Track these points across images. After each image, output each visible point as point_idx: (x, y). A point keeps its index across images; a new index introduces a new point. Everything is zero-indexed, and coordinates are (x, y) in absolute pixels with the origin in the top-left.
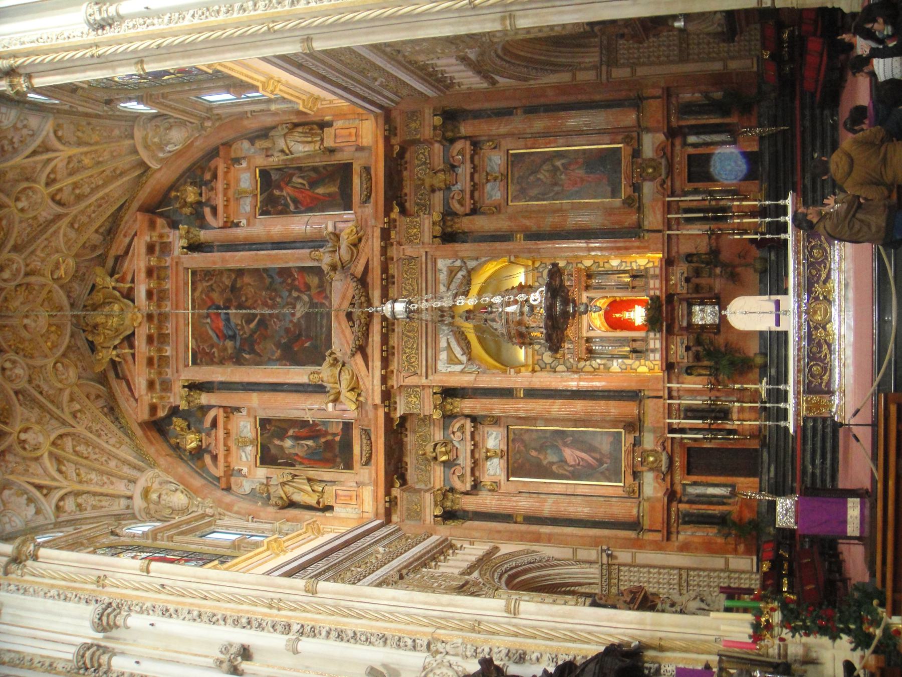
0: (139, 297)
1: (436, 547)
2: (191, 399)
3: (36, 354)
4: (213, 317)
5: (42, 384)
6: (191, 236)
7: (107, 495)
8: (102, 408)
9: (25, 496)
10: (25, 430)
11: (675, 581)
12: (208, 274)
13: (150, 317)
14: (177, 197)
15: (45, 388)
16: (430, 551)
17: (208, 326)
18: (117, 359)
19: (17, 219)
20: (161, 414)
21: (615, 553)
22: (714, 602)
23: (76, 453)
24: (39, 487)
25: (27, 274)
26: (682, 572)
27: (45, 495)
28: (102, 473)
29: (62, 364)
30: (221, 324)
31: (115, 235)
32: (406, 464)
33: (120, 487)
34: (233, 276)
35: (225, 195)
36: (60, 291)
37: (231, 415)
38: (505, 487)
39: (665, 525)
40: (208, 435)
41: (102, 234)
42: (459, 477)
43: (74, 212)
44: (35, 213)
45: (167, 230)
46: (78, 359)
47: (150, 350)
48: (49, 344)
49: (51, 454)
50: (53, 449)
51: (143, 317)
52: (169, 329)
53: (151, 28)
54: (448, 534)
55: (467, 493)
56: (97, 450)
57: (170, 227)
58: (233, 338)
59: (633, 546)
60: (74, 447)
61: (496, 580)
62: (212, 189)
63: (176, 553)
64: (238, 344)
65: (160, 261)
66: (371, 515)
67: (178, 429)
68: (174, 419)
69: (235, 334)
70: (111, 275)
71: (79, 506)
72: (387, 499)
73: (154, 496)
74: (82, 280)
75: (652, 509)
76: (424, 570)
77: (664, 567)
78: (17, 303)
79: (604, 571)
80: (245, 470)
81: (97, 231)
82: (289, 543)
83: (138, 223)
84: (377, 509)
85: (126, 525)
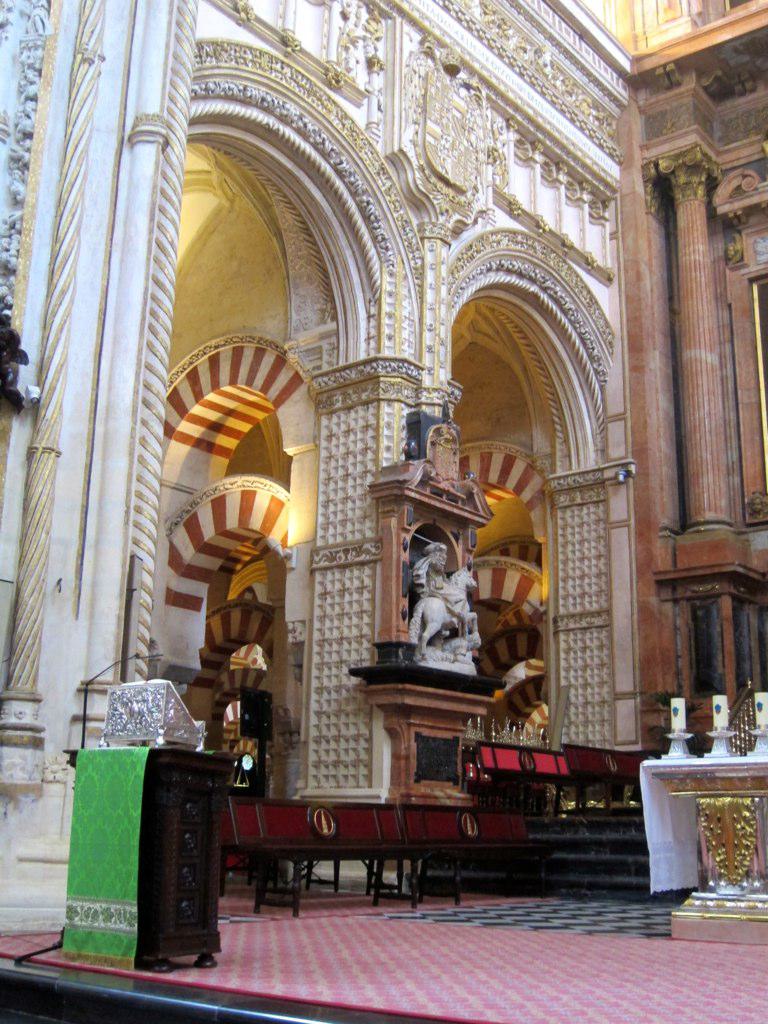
1: (584, 166)
11: (587, 606)
16: (568, 153)
21: (623, 489)
22: (454, 651)
26: (604, 616)
32: (753, 90)
38: (736, 279)
39: (685, 574)
42: (739, 187)
54: (625, 191)
55: (711, 214)
59: (638, 521)
61: (506, 264)
66: (643, 50)
72: (671, 67)
75: (716, 546)
76: (513, 136)
77: (609, 583)
79: (590, 476)
84: (650, 55)
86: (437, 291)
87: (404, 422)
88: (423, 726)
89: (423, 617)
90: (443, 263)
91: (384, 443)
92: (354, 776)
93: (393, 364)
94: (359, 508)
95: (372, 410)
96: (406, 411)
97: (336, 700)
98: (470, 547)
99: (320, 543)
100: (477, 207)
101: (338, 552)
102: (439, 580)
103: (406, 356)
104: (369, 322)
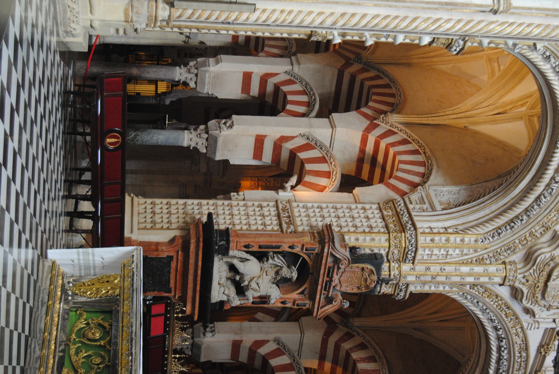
86: (469, 275)
87: (376, 251)
88: (177, 262)
89: (248, 260)
90: (490, 278)
91: (361, 237)
92: (146, 221)
93: (413, 240)
94: (317, 224)
95: (382, 230)
96: (383, 252)
97: (193, 212)
98: (296, 302)
99: (294, 204)
100: (536, 309)
101: (288, 213)
102: (272, 273)
103: (420, 251)
104: (442, 228)
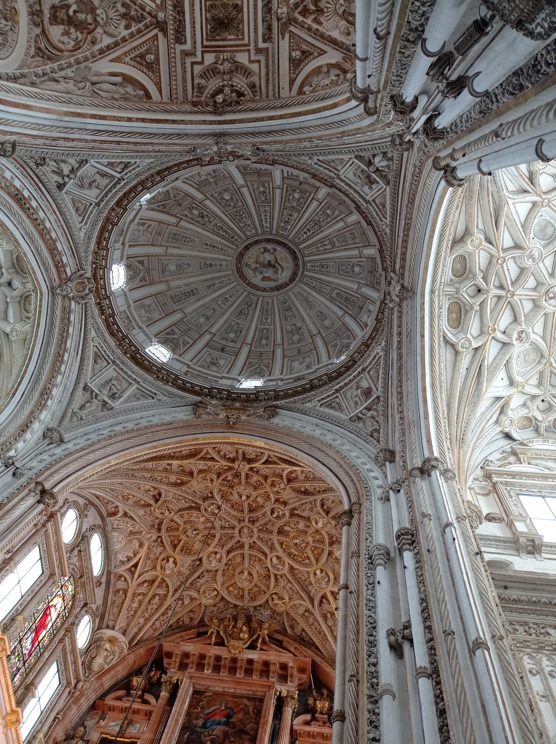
0: (249, 653)
2: (168, 684)
3: (225, 578)
4: (225, 712)
5: (204, 579)
6: (289, 699)
7: (120, 612)
8: (183, 621)
9: (133, 556)
10: (175, 563)
12: (259, 712)
13: (234, 660)
14: (322, 695)
15: (202, 581)
17: (218, 706)
18: (210, 632)
19: (309, 570)
20: (166, 661)
23: (154, 596)
24: (136, 566)
25: (276, 575)
27: (129, 570)
28: (136, 612)
29: (217, 595)
30: (217, 718)
31: (299, 642)
33: (121, 623)
34: (252, 733)
35: (318, 733)
36: (264, 600)
37: (148, 718)
40: (139, 697)
41: (301, 634)
43: (314, 612)
44: (313, 582)
45: (297, 682)
46: (219, 608)
47: (210, 657)
48: (231, 588)
49: (158, 577)
50: (160, 579)
51: (235, 654)
52: (224, 674)
53: (365, 588)
56: (153, 611)
57: (300, 685)
58: (204, 726)
60: (159, 595)
62: (324, 723)
63: (46, 640)
64: (199, 730)
65: (273, 673)
67: (152, 674)
68: (159, 673)
69: (207, 728)
70: (269, 637)
71: (118, 591)
73: (108, 646)
74: (271, 618)
78: (258, 568)
80: (102, 723)
81: (303, 630)
82: (14, 736)
83: (302, 658)
85: (94, 621)
